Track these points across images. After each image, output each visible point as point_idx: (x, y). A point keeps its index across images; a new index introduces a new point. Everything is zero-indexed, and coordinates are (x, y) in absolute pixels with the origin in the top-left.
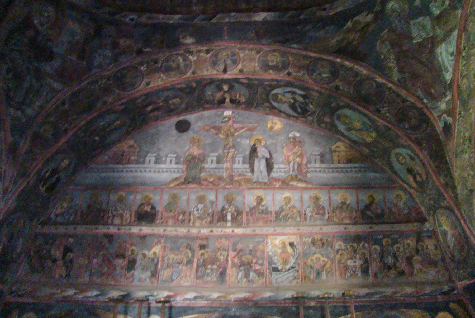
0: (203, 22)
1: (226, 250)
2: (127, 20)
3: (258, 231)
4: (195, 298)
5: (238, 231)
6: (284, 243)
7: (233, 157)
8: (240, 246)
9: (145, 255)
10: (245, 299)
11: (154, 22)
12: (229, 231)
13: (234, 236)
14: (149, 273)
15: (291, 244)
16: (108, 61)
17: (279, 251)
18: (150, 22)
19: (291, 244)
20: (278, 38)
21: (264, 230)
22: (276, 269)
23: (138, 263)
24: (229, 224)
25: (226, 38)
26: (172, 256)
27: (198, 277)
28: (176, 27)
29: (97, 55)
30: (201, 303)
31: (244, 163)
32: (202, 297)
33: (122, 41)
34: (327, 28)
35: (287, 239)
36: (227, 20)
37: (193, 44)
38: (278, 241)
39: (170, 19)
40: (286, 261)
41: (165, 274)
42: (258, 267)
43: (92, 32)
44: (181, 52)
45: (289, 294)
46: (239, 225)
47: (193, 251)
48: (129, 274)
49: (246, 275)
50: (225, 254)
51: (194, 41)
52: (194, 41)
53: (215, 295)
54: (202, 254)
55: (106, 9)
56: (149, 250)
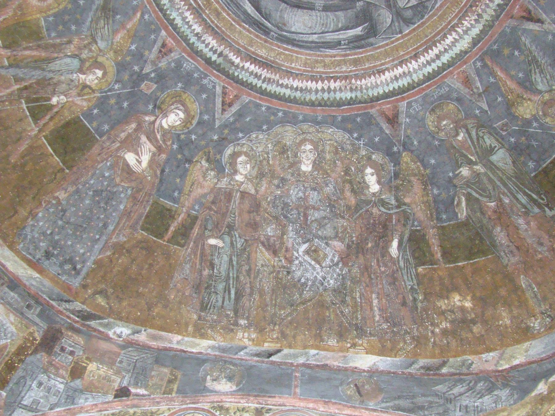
0: (256, 358)
2: (111, 333)
11: (162, 344)
16: (53, 400)
18: (154, 344)
20: (402, 403)
25: (298, 390)
28: (200, 360)
29: (34, 385)
33: (92, 367)
34: (495, 393)
36: (301, 360)
37: (232, 394)
39: (195, 345)
43: (38, 337)
44: (207, 406)
51: (234, 388)
52: (234, 388)
55: (78, 306)
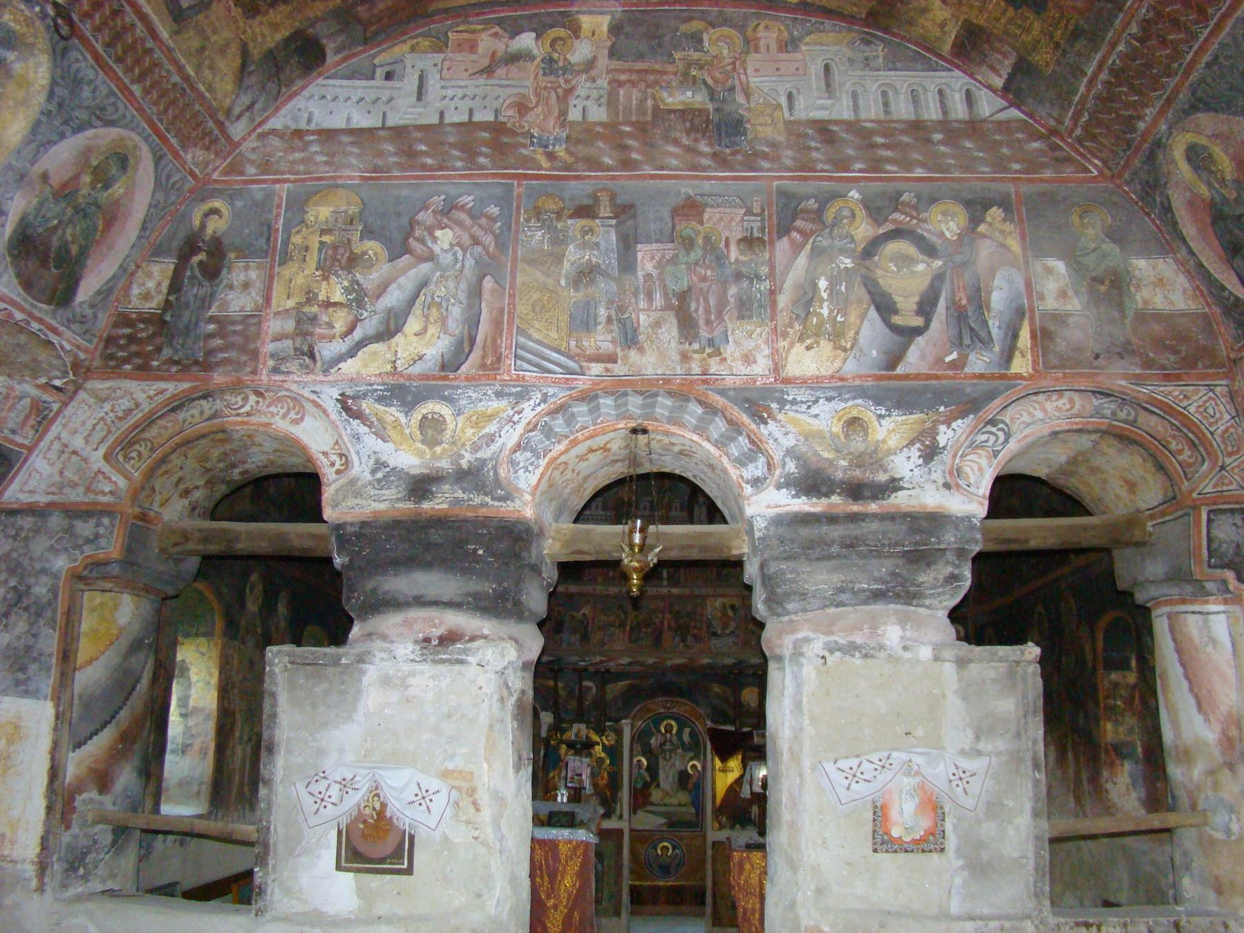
1: (662, 612)
3: (697, 591)
4: (630, 663)
5: (675, 591)
6: (724, 606)
7: (670, 503)
8: (676, 608)
9: (573, 617)
10: (684, 666)
12: (665, 591)
13: (669, 596)
14: (578, 636)
15: (733, 607)
17: (719, 614)
19: (733, 607)
21: (704, 591)
22: (715, 634)
23: (566, 625)
24: (665, 583)
26: (603, 617)
27: (631, 641)
30: (638, 668)
31: (682, 510)
32: (637, 663)
35: (727, 601)
38: (718, 603)
40: (725, 626)
41: (596, 637)
42: (695, 632)
45: (729, 661)
46: (676, 585)
47: (625, 613)
48: (557, 638)
49: (683, 640)
50: (660, 616)
53: (651, 661)
54: (636, 617)
56: (578, 611)
